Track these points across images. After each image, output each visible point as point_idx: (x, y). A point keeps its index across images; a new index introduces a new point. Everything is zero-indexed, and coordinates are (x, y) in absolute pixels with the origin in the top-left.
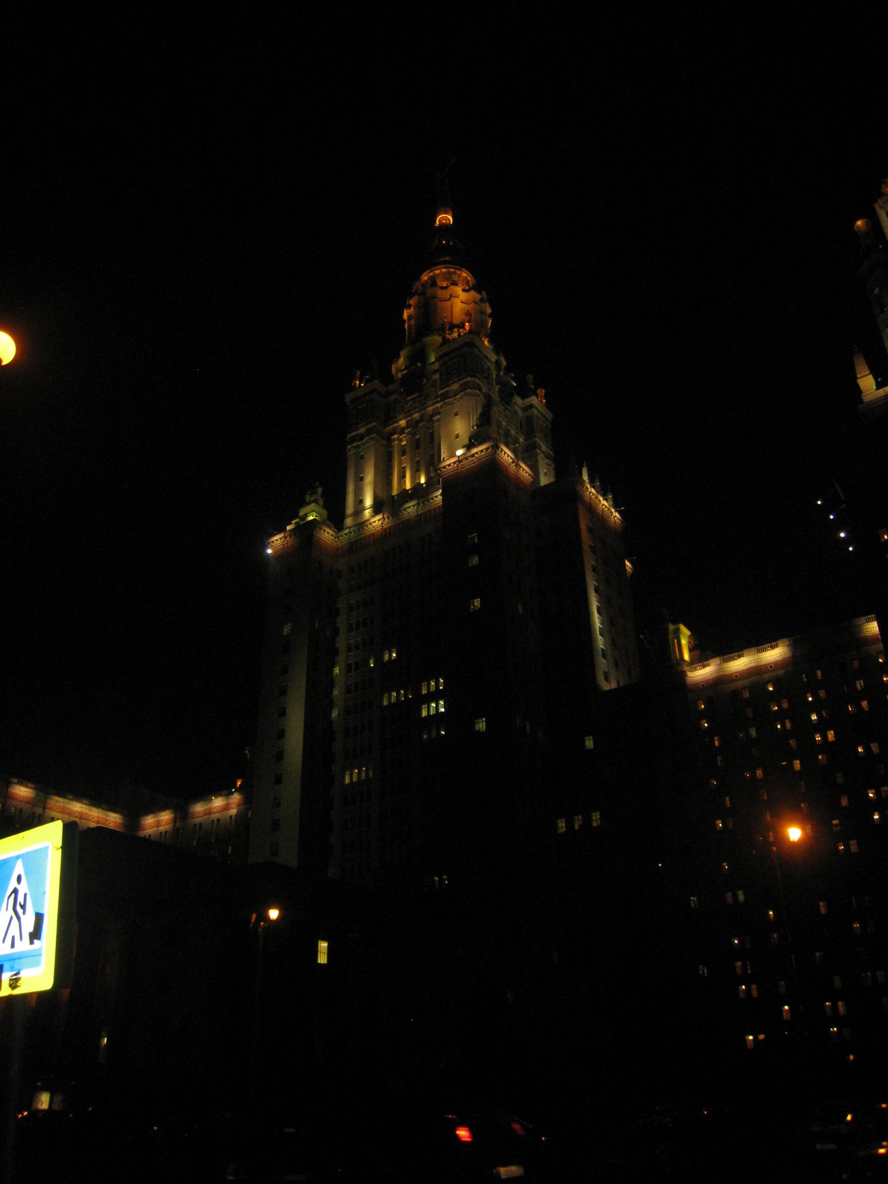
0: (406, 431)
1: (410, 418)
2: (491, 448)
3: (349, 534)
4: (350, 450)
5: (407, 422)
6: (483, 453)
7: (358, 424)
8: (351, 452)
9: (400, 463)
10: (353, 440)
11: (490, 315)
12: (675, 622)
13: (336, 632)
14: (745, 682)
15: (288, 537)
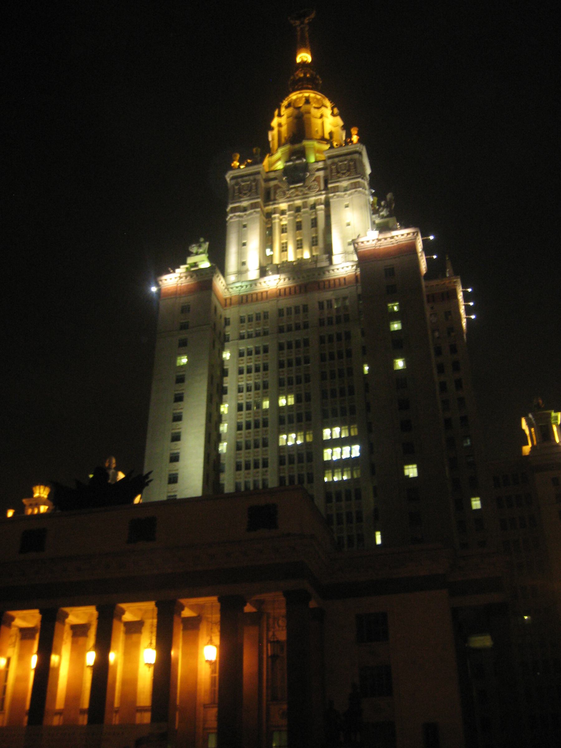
2: (411, 234)
3: (240, 288)
4: (231, 218)
5: (289, 206)
6: (403, 237)
10: (234, 210)
15: (184, 278)
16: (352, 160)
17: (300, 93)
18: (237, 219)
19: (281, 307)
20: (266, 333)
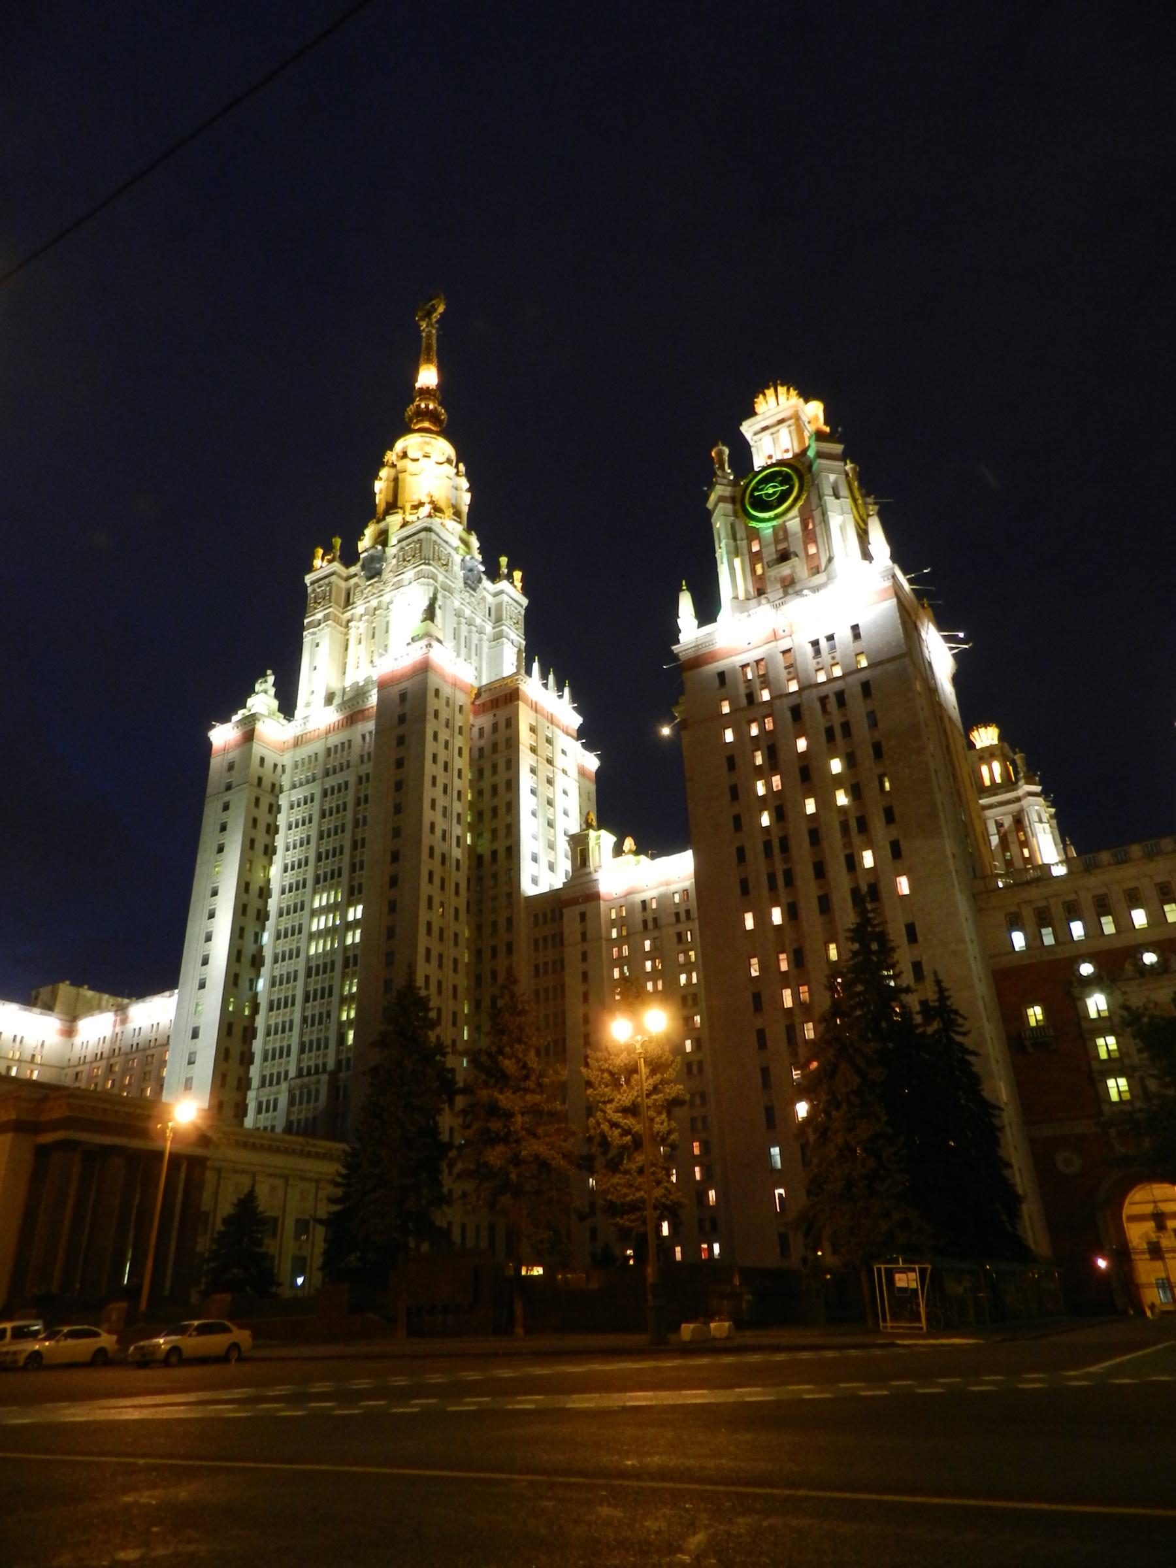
0: (364, 618)
1: (367, 605)
5: (366, 608)
7: (315, 608)
11: (469, 490)
12: (599, 827)
16: (420, 541)
18: (311, 637)
19: (329, 746)
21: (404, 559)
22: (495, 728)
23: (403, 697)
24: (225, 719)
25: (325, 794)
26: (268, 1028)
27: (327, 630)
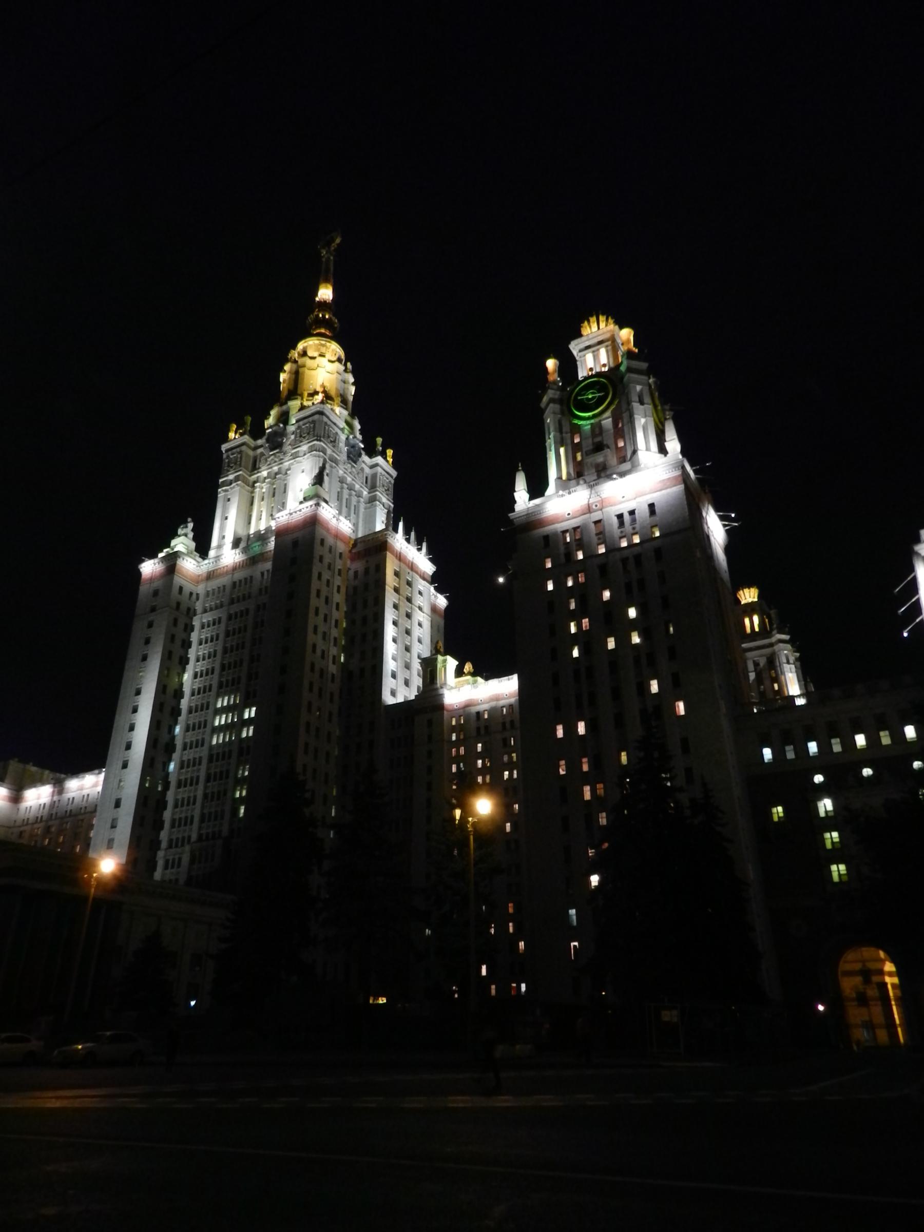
0: (266, 481)
1: (270, 470)
2: (314, 506)
3: (208, 565)
5: (268, 473)
6: (308, 509)
7: (229, 471)
8: (221, 495)
9: (260, 506)
11: (353, 384)
12: (445, 654)
13: (189, 645)
14: (486, 706)
15: (157, 564)
16: (314, 422)
17: (305, 342)
18: (223, 494)
19: (235, 580)
20: (222, 606)
21: (301, 436)
22: (367, 571)
23: (295, 543)
24: (153, 556)
25: (230, 618)
26: (176, 801)
27: (237, 488)
